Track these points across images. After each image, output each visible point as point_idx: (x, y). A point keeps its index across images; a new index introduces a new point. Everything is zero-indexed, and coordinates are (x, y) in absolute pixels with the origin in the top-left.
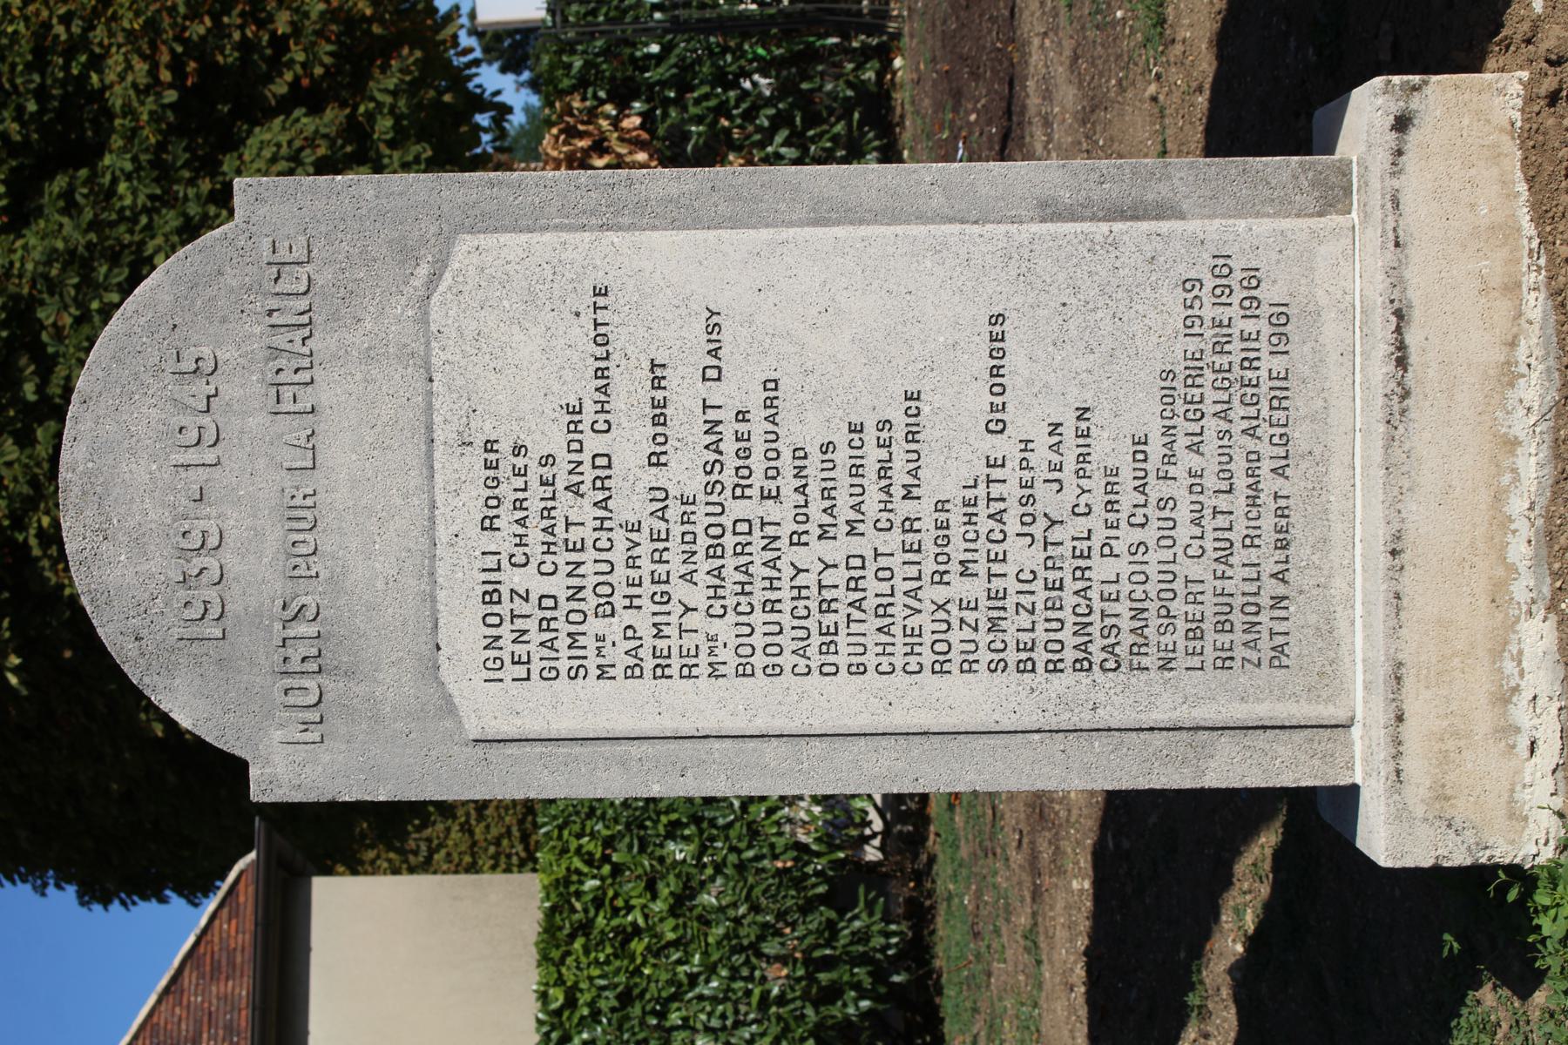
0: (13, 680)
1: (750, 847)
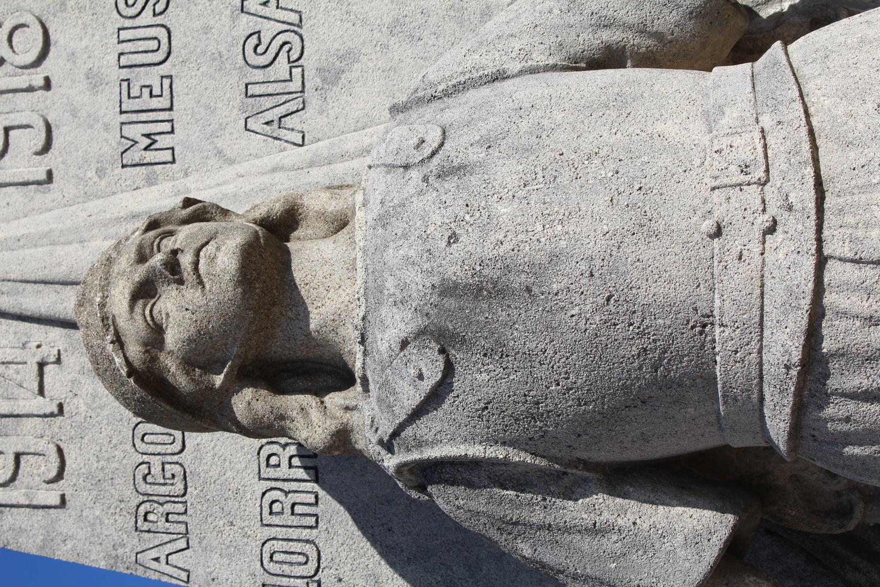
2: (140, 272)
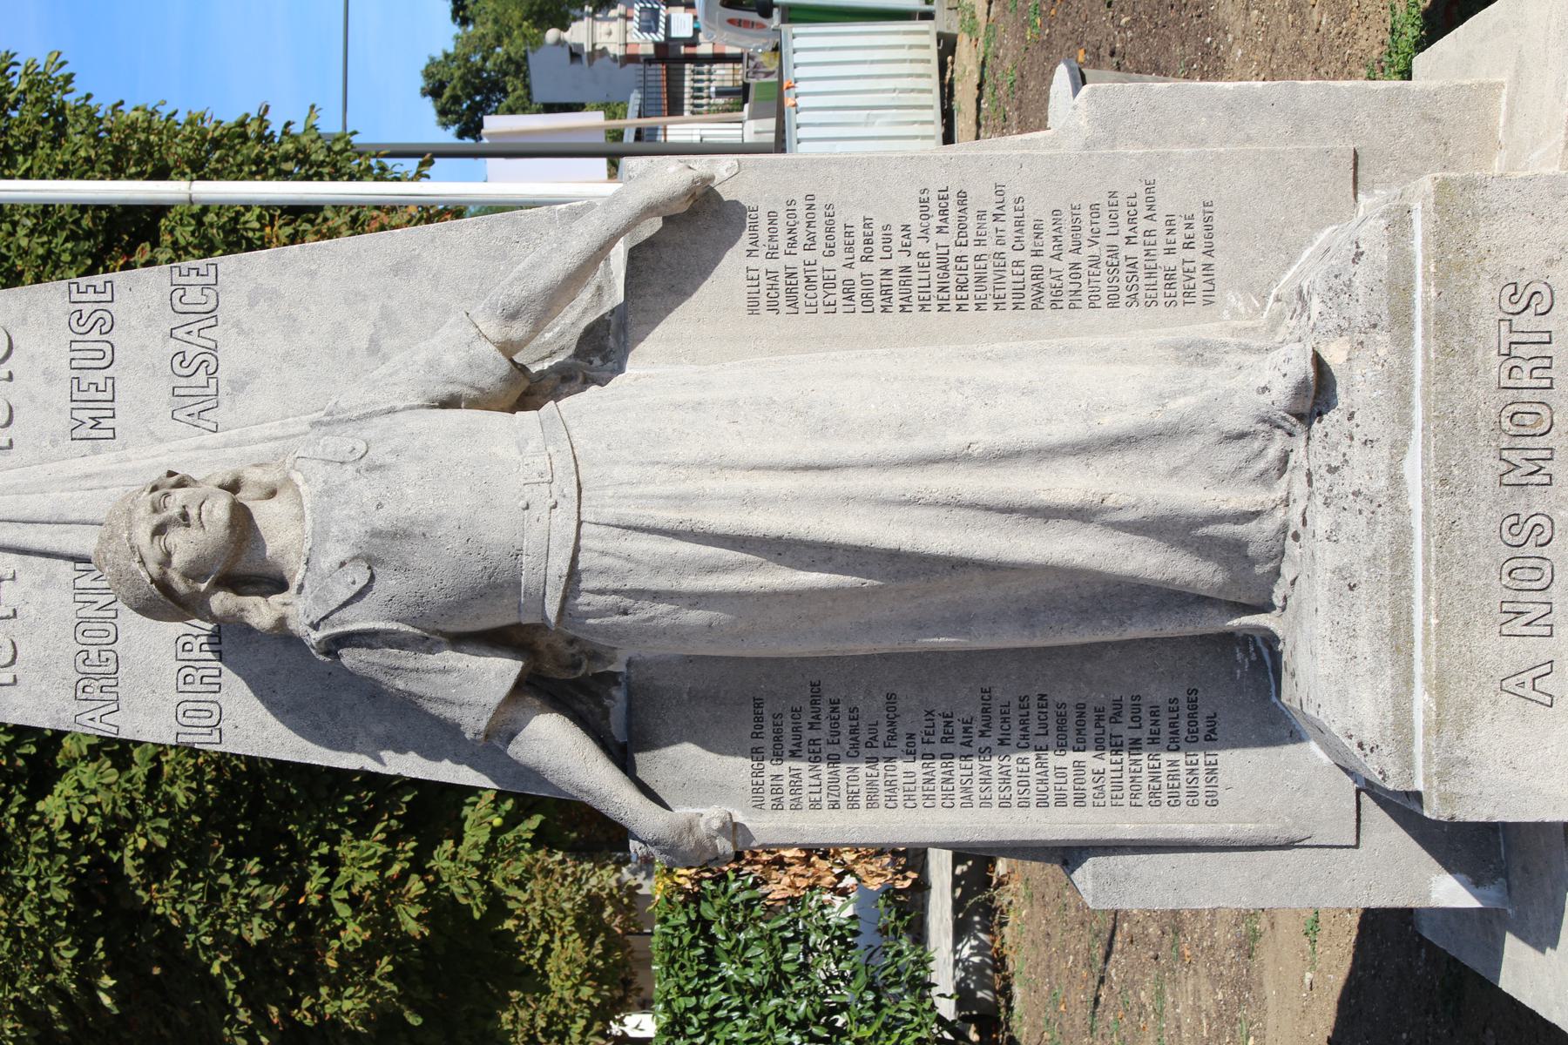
0: (106, 1000)
2: (157, 519)
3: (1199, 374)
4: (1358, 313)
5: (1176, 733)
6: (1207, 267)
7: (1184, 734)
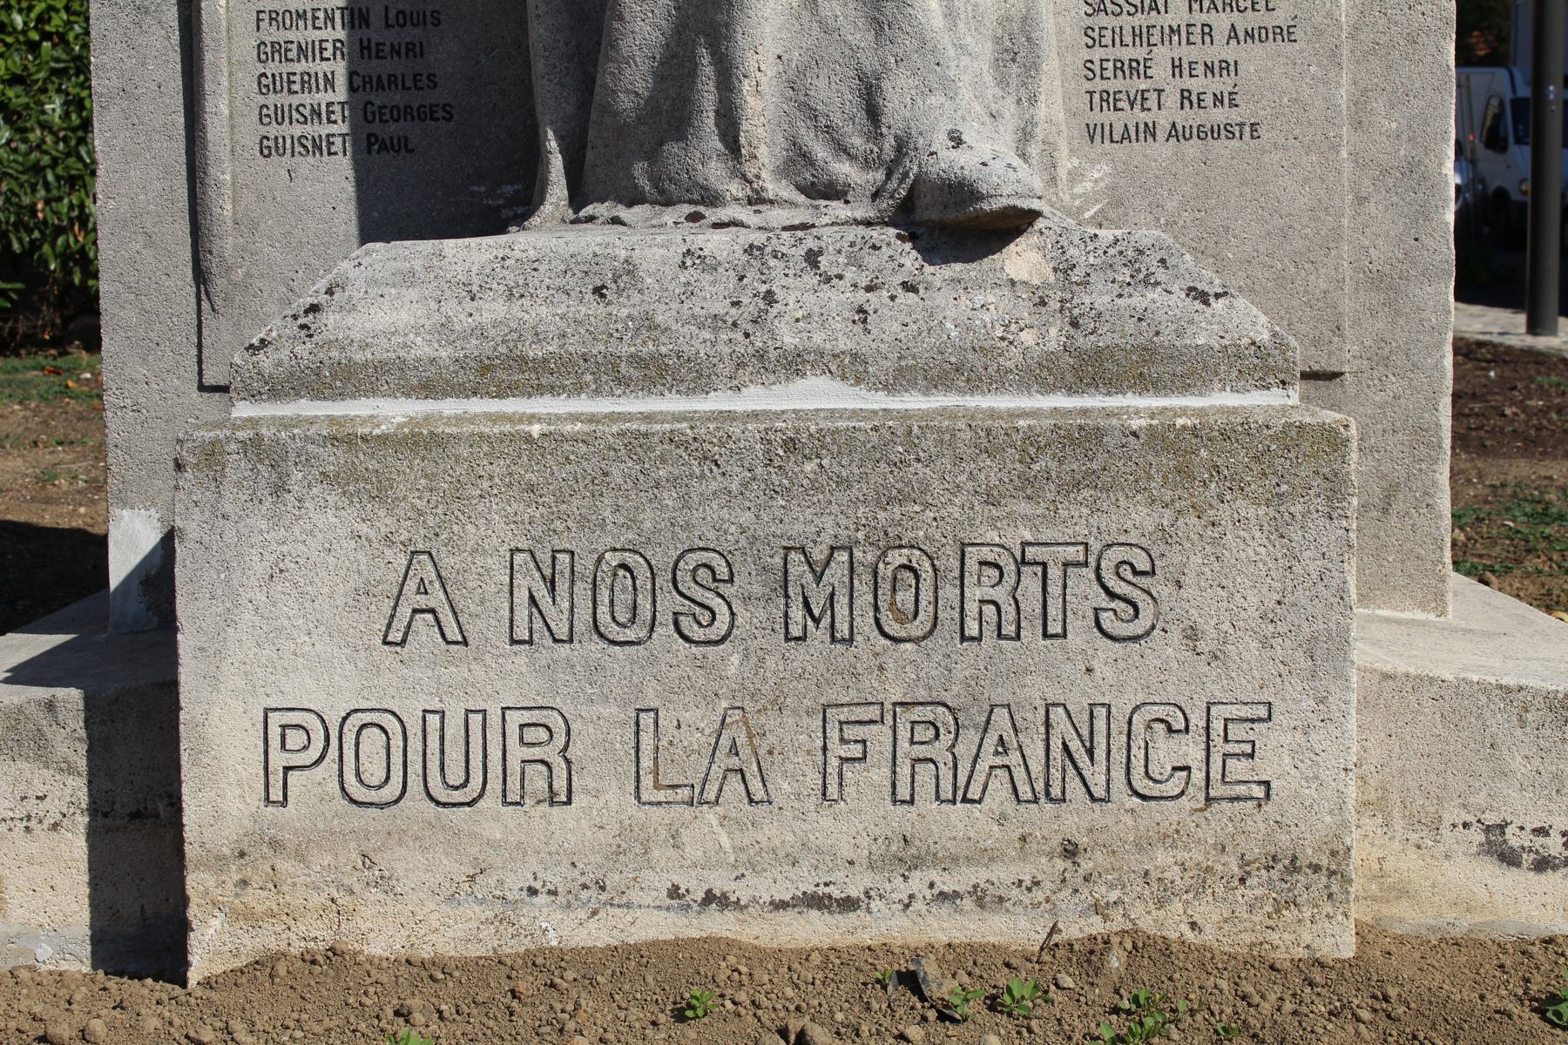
1: (58, 178)
3: (986, 49)
4: (1099, 297)
5: (380, 86)
6: (1150, 131)
7: (378, 99)
